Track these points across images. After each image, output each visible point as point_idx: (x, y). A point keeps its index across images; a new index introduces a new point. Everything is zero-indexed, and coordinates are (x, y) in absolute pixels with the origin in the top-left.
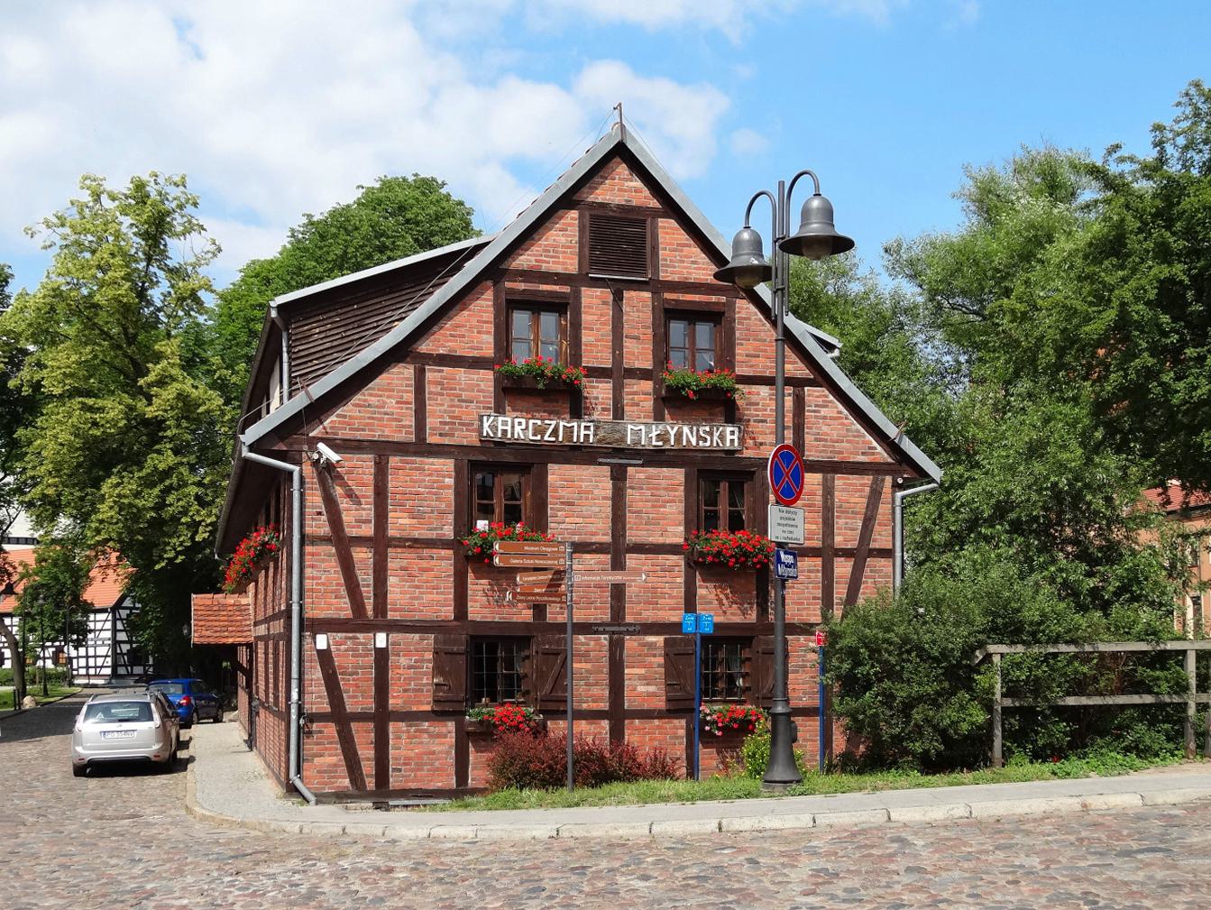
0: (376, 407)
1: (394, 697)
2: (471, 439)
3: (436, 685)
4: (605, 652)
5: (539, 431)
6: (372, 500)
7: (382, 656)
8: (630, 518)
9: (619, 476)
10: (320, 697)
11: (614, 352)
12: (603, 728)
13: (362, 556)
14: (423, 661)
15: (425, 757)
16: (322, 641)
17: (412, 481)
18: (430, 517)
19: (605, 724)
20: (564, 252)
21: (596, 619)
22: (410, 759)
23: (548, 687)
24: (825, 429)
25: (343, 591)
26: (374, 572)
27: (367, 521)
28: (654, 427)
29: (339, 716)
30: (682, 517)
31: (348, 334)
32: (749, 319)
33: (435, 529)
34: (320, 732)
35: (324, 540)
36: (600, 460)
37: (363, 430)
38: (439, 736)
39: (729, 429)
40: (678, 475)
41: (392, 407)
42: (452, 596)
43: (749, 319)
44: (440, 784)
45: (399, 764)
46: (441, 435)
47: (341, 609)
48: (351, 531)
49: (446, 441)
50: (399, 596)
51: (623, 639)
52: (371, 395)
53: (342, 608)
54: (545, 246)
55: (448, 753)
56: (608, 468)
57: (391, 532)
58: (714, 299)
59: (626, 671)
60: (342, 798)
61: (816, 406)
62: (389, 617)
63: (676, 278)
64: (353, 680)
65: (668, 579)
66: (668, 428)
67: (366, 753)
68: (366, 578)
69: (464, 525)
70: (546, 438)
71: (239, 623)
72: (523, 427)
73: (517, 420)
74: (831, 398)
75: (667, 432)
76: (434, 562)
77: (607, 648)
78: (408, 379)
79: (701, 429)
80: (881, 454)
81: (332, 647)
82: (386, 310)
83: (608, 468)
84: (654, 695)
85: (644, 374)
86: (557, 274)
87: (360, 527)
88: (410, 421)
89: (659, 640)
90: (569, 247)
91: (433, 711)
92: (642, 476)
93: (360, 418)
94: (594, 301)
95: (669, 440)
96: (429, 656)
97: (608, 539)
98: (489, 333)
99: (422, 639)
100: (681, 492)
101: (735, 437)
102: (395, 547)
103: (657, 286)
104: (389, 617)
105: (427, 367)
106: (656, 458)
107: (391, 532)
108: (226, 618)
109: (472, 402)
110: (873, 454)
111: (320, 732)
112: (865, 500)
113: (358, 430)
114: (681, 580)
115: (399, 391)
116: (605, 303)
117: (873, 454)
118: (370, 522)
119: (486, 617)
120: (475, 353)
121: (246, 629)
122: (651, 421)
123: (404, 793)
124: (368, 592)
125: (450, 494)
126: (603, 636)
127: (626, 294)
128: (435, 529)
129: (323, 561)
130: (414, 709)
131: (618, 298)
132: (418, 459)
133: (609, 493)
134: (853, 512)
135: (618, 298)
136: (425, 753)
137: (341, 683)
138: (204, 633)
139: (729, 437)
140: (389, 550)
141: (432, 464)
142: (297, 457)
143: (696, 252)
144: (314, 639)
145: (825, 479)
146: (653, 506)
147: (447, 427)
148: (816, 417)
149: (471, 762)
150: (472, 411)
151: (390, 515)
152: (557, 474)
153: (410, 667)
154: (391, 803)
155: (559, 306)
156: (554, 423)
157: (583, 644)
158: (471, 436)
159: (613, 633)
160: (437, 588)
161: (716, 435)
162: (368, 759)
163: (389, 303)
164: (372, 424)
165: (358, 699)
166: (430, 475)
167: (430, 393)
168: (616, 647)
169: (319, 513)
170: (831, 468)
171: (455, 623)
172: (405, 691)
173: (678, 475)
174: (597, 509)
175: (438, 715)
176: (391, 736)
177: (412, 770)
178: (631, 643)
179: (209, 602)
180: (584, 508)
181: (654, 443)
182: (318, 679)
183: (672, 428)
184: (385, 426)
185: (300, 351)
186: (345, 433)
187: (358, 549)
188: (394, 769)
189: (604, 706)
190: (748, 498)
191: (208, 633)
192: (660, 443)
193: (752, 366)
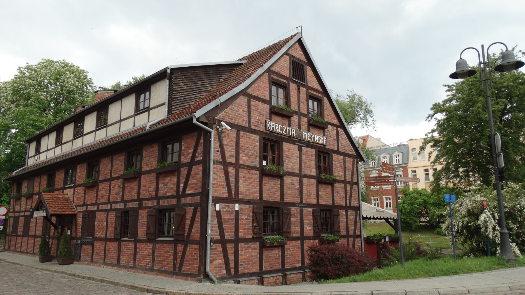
0: (237, 111)
1: (241, 232)
2: (262, 128)
3: (254, 226)
4: (299, 214)
5: (282, 129)
6: (235, 148)
7: (237, 213)
8: (303, 165)
9: (300, 150)
10: (216, 232)
11: (298, 106)
12: (299, 244)
13: (231, 170)
14: (249, 216)
15: (250, 258)
16: (218, 207)
17: (247, 142)
18: (252, 157)
19: (299, 242)
20: (286, 69)
21: (296, 201)
22: (245, 259)
23: (286, 227)
24: (343, 142)
25: (225, 186)
26: (235, 178)
27: (233, 156)
29: (223, 241)
30: (315, 166)
31: (192, 85)
32: (327, 103)
33: (253, 162)
34: (216, 248)
35: (219, 163)
36: (296, 143)
37: (232, 119)
38: (255, 249)
39: (325, 138)
40: (313, 151)
41: (241, 112)
42: (258, 190)
43: (327, 103)
44: (254, 270)
45: (242, 262)
46: (255, 126)
47: (224, 193)
48: (228, 160)
49: (256, 128)
50: (243, 188)
51: (303, 210)
52: (235, 106)
53: (223, 193)
54: (282, 66)
55: (257, 256)
56: (297, 146)
57: (241, 162)
58: (320, 95)
59: (304, 221)
60: (223, 279)
61: (341, 134)
62: (239, 198)
63: (311, 86)
64: (228, 224)
65: (312, 188)
67: (231, 257)
68: (232, 180)
69: (261, 163)
70: (284, 133)
71: (67, 206)
72: (278, 127)
73: (276, 125)
74: (344, 133)
76: (253, 175)
77: (299, 213)
78: (245, 102)
80: (354, 153)
81: (221, 210)
82: (205, 79)
83: (297, 146)
84: (310, 230)
85: (305, 116)
86: (284, 76)
87: (231, 158)
88: (246, 119)
89: (310, 210)
90: (287, 68)
91: (253, 238)
92: (305, 150)
93: (231, 114)
94: (293, 87)
96: (251, 214)
97: (298, 172)
98: (267, 91)
99: (250, 207)
100: (314, 158)
101: (326, 141)
102: (242, 168)
103: (308, 88)
104: (239, 198)
105: (251, 99)
106: (310, 145)
107: (241, 162)
108: (61, 203)
109: (263, 115)
110: (352, 152)
111: (216, 248)
112: (351, 166)
113: (231, 119)
114: (315, 188)
115: (243, 107)
116: (296, 89)
117: (352, 152)
118: (233, 156)
119: (268, 199)
120: (264, 98)
121: (72, 208)
122: (307, 131)
123: (244, 275)
124: (233, 186)
125: (257, 149)
126: (298, 208)
127: (301, 88)
128: (253, 162)
129: (219, 171)
130: (247, 237)
131: (299, 89)
132: (249, 134)
133: (298, 155)
134: (350, 170)
135: (299, 89)
136: (249, 257)
137: (224, 226)
138: (54, 209)
139: (325, 141)
140: (240, 169)
141: (253, 136)
142: (211, 126)
143: (314, 78)
144: (215, 205)
145: (344, 158)
146: (308, 161)
147: (257, 123)
148: (341, 138)
149: (264, 259)
150: (263, 119)
151: (241, 155)
152: (286, 146)
153: (246, 219)
154: (241, 279)
155: (285, 87)
156: (285, 127)
157: (293, 211)
158: (263, 128)
159: (300, 207)
160: (253, 186)
161: (322, 139)
162: (232, 260)
163: (205, 77)
164: (235, 118)
165: (229, 235)
166: (252, 141)
167: (252, 109)
168: (301, 212)
169: (218, 151)
170: (345, 155)
171: (259, 201)
172: (244, 229)
173: (313, 151)
174: (295, 161)
175: (253, 240)
176: (240, 249)
177: (246, 264)
178: (305, 211)
179: (51, 196)
180: (293, 160)
181: (309, 140)
182: (216, 224)
184: (239, 119)
185: (176, 88)
186: (227, 120)
187: (230, 168)
188: (240, 264)
189: (299, 235)
190: (327, 162)
191: (55, 209)
192: (310, 140)
193: (328, 119)
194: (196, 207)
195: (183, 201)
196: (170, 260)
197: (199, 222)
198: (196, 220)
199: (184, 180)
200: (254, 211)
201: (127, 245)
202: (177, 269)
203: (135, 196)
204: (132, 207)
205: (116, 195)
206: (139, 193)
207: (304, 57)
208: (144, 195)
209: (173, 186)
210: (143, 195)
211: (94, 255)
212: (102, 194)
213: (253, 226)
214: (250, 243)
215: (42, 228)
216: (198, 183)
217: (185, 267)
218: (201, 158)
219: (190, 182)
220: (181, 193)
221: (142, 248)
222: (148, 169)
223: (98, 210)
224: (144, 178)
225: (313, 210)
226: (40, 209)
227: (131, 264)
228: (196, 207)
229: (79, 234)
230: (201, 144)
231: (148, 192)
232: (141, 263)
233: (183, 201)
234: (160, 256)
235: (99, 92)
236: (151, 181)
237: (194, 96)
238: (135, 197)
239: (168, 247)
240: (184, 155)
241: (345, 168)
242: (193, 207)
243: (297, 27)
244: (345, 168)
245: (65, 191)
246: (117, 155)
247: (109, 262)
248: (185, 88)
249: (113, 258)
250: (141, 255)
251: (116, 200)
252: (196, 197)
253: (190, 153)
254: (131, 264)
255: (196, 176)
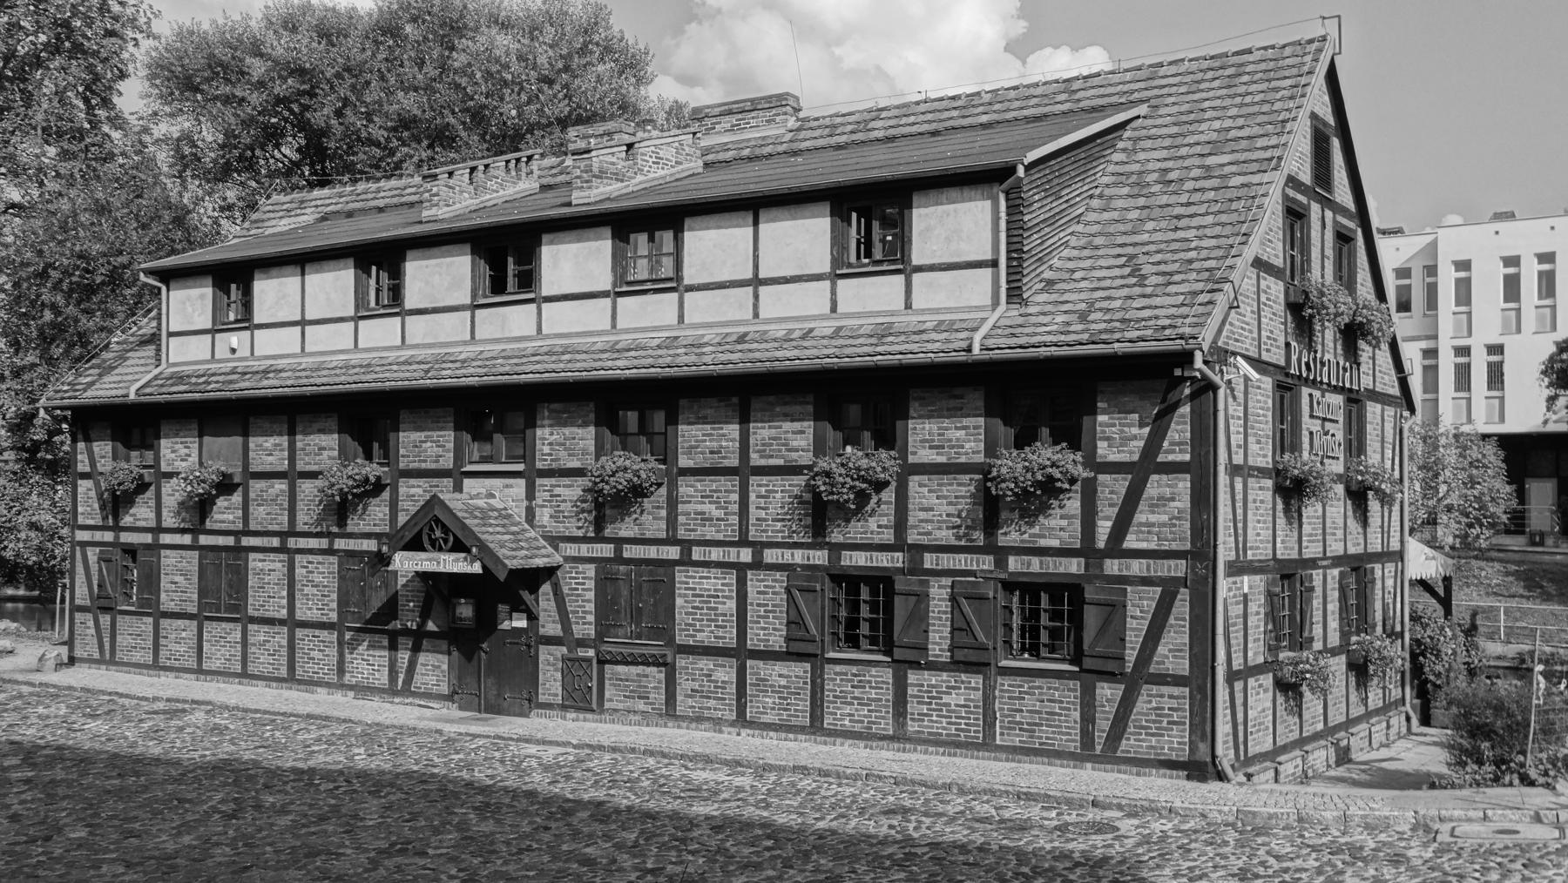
80: (1395, 391)
194: (1169, 590)
195: (1112, 567)
196: (1066, 721)
197: (1187, 629)
198: (1172, 621)
199: (1116, 510)
200: (1269, 591)
201: (855, 675)
202: (1098, 748)
203: (879, 533)
204: (869, 564)
205: (779, 524)
206: (900, 525)
207: (1330, 110)
208: (929, 533)
209: (1064, 523)
210: (919, 534)
211: (679, 698)
212: (704, 513)
213: (1265, 633)
214: (1262, 677)
215: (335, 596)
216: (1175, 525)
217: (1132, 742)
218: (1187, 457)
219: (1140, 517)
220: (1101, 544)
221: (933, 686)
222: (942, 459)
223: (686, 561)
224: (921, 485)
225: (1341, 573)
226: (427, 545)
227: (887, 726)
228: (1169, 590)
229: (585, 627)
230: (1183, 416)
231: (948, 528)
232: (932, 727)
233: (1112, 567)
234: (1022, 711)
235: (593, 153)
236: (956, 497)
237: (1056, 238)
238: (888, 536)
239: (1056, 689)
240: (1108, 439)
241: (1383, 441)
242: (1159, 589)
243: (1324, 18)
244: (1383, 441)
245: (467, 482)
246: (771, 398)
247: (766, 719)
248: (1042, 217)
249: (785, 710)
250: (930, 703)
251: (783, 537)
252: (1172, 562)
253: (1135, 437)
254: (884, 729)
255: (1165, 505)
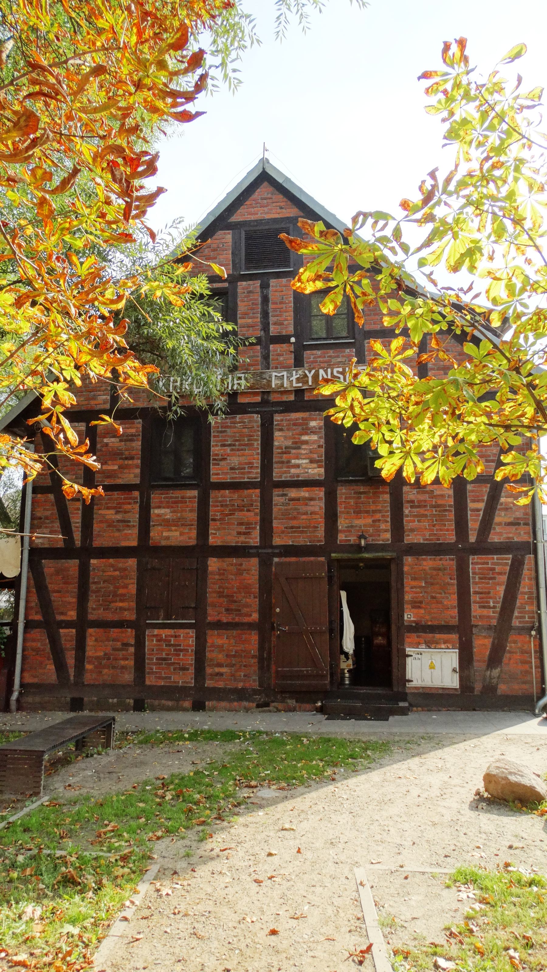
28: (294, 372)
66: (307, 372)
75: (306, 376)
79: (335, 370)
95: (308, 382)
181: (295, 385)
183: (310, 372)
192: (300, 385)
